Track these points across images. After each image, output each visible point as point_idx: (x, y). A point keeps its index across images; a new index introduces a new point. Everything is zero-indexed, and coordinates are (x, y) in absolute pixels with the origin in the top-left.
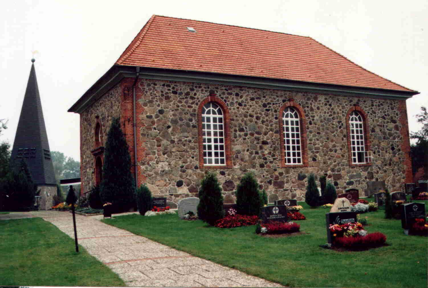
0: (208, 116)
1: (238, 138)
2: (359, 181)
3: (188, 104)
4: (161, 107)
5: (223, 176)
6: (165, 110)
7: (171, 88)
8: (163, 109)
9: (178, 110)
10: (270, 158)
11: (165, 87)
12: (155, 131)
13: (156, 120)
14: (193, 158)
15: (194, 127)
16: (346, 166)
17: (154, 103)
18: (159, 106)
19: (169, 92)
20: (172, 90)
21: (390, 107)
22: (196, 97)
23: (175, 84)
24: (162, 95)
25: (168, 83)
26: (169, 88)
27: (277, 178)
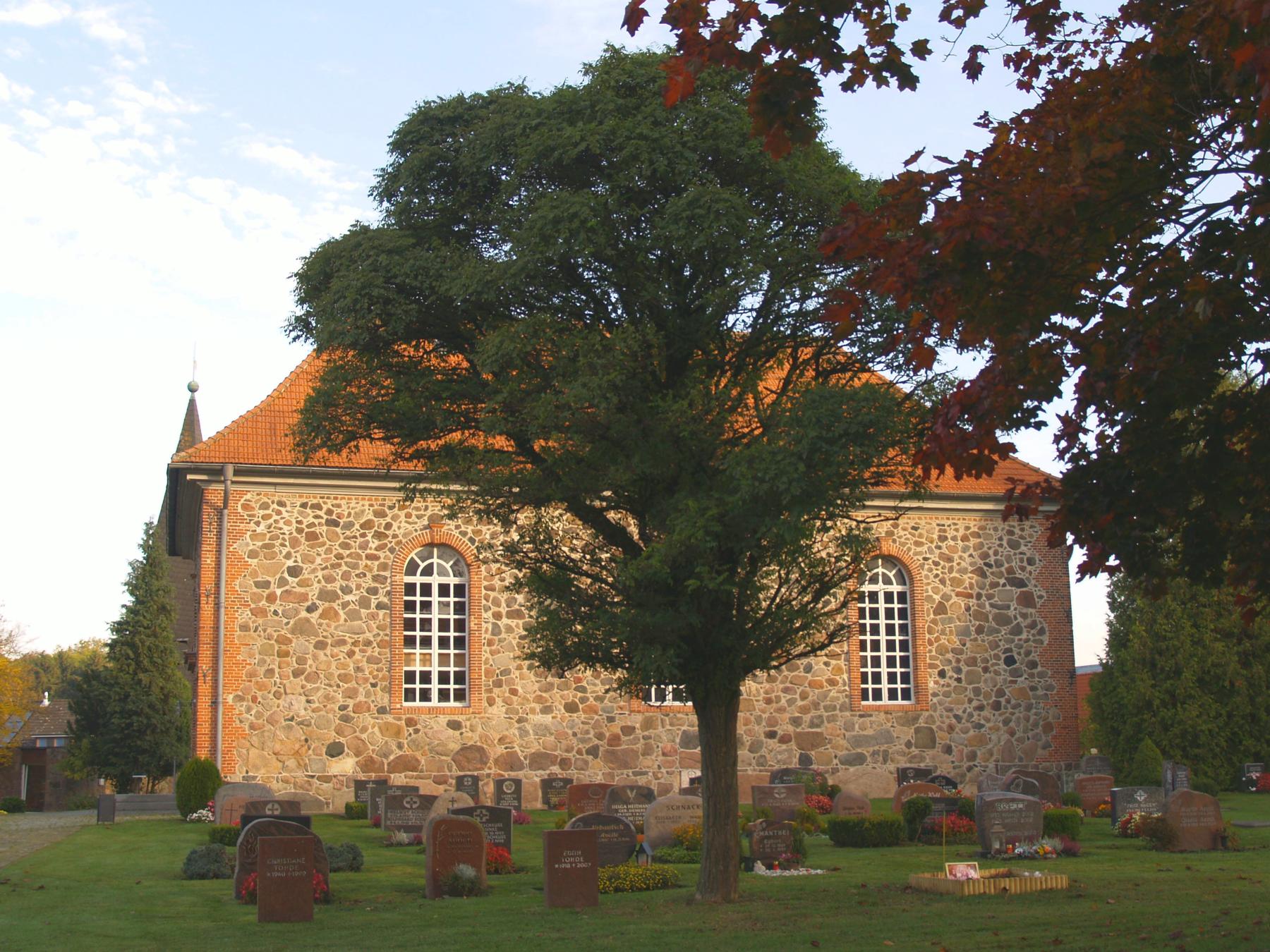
0: (426, 580)
1: (503, 635)
2: (886, 753)
3: (368, 551)
4: (293, 559)
5: (457, 733)
6: (305, 566)
7: (321, 513)
8: (301, 564)
9: (339, 565)
10: (597, 689)
11: (308, 510)
12: (276, 618)
13: (279, 592)
14: (374, 685)
15: (380, 606)
16: (841, 710)
17: (276, 549)
18: (288, 556)
19: (316, 521)
20: (325, 517)
21: (1005, 543)
22: (390, 533)
23: (335, 502)
24: (300, 531)
25: (315, 501)
26: (319, 513)
27: (615, 740)
